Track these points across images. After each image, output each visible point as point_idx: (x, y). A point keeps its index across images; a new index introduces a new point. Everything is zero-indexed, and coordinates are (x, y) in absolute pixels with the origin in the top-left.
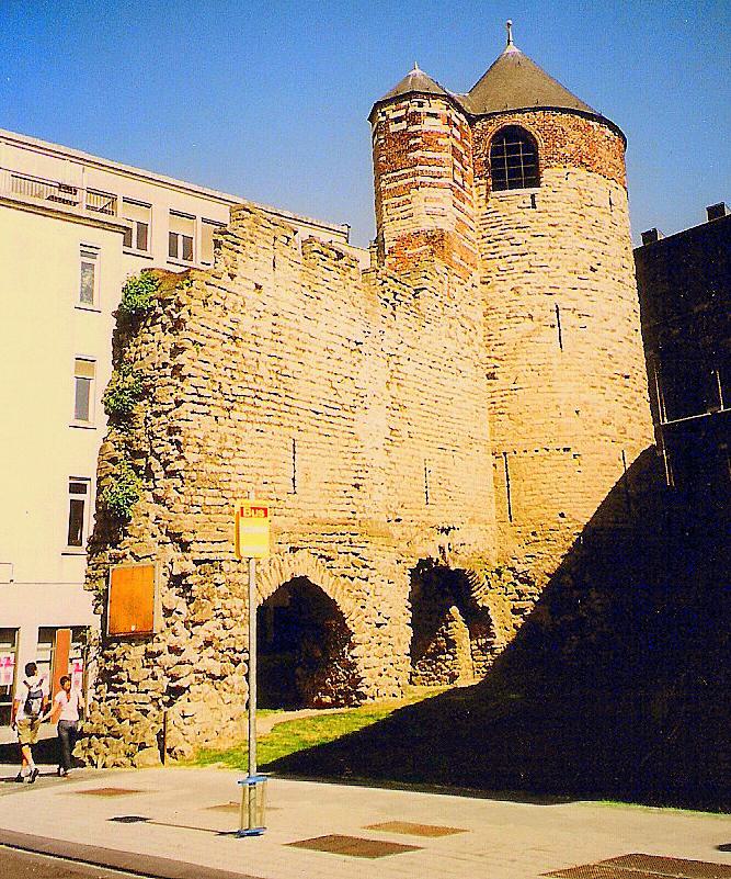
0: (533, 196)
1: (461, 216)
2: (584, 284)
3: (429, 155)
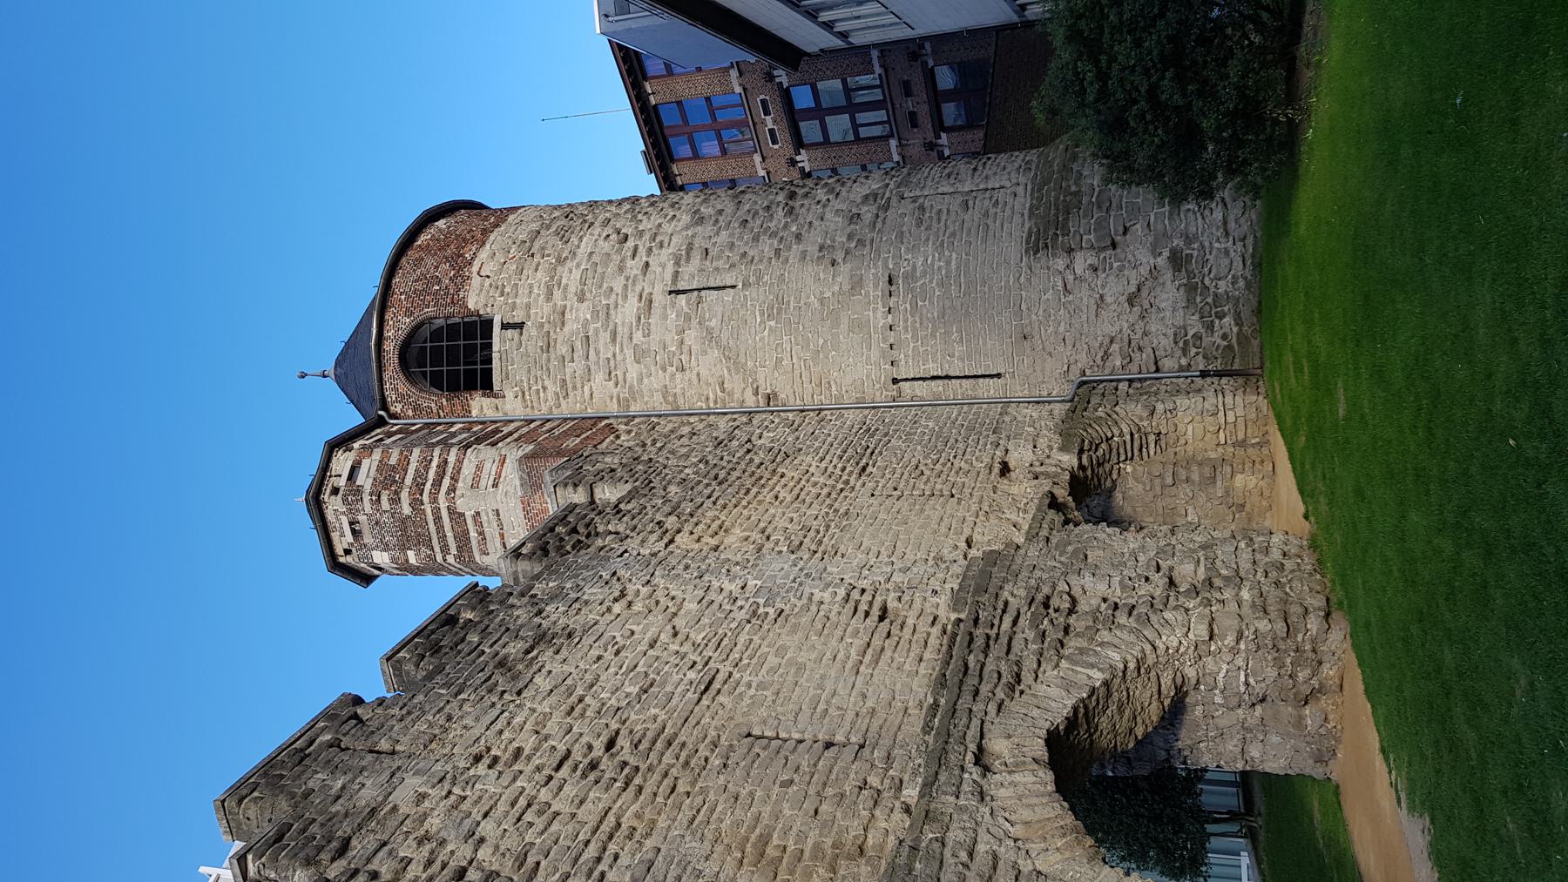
0: (505, 326)
1: (516, 435)
2: (642, 250)
3: (409, 480)
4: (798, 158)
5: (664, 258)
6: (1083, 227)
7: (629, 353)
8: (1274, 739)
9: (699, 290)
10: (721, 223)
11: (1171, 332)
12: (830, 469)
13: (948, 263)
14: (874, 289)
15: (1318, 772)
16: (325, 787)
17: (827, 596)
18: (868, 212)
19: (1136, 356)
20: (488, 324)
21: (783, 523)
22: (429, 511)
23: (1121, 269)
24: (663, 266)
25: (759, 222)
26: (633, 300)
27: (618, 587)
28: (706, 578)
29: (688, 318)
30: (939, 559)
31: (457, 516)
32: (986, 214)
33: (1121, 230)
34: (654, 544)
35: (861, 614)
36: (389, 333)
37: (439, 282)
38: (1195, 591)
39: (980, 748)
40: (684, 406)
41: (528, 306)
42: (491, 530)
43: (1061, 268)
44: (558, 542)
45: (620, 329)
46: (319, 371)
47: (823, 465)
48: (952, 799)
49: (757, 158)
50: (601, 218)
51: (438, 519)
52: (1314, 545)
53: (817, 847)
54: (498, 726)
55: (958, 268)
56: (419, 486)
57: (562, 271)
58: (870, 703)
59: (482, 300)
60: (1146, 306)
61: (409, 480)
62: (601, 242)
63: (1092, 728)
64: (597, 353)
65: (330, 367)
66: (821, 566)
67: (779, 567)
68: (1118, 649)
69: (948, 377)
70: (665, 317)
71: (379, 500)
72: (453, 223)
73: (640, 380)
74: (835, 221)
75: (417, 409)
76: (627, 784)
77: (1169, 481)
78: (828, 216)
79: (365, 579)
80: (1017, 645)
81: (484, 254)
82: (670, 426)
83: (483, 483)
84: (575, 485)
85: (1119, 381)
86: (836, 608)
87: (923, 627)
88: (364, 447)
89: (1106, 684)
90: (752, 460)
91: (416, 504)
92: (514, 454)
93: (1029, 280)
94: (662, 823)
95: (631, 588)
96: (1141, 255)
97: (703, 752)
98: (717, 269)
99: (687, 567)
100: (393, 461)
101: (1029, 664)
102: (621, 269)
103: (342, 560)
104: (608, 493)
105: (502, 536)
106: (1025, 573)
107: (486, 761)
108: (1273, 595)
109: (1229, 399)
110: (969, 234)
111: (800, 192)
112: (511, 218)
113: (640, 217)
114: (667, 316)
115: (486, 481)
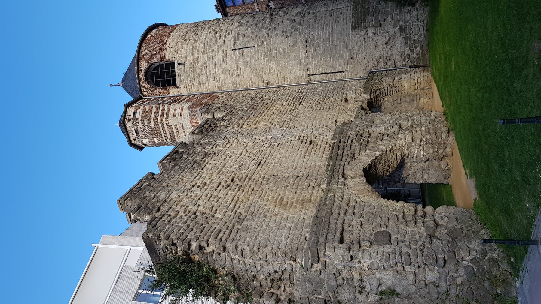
0: (179, 64)
2: (222, 36)
3: (153, 116)
4: (270, 4)
5: (230, 38)
6: (370, 20)
7: (220, 71)
8: (432, 172)
9: (242, 48)
10: (249, 25)
11: (400, 54)
12: (290, 104)
13: (325, 34)
14: (301, 44)
15: (445, 182)
17: (293, 139)
18: (298, 18)
19: (388, 62)
20: (172, 65)
21: (276, 120)
22: (160, 125)
23: (383, 33)
24: (230, 41)
25: (261, 24)
27: (227, 140)
28: (254, 136)
29: (239, 58)
30: (327, 127)
31: (169, 126)
32: (338, 17)
33: (383, 20)
34: (236, 128)
35: (304, 143)
37: (156, 51)
38: (407, 129)
39: (343, 173)
40: (239, 88)
41: (186, 57)
42: (181, 130)
43: (363, 34)
44: (206, 129)
45: (217, 63)
46: (116, 84)
47: (287, 103)
48: (336, 186)
49: (256, 5)
51: (163, 127)
52: (445, 114)
53: (297, 201)
54: (198, 177)
55: (329, 36)
56: (156, 117)
57: (197, 45)
58: (309, 165)
59: (171, 56)
60: (392, 45)
61: (153, 116)
62: (208, 34)
63: (376, 169)
65: (120, 82)
66: (290, 131)
67: (277, 132)
68: (384, 146)
69: (326, 73)
70: (232, 58)
71: (144, 122)
72: (157, 32)
73: (225, 80)
74: (287, 22)
75: (152, 93)
76: (239, 190)
77: (399, 102)
78: (284, 21)
80: (353, 147)
81: (170, 40)
82: (236, 94)
83: (177, 115)
84: (208, 113)
85: (383, 71)
86: (296, 142)
87: (323, 145)
88: (137, 106)
89: (381, 155)
90: (264, 103)
91: (156, 123)
92: (186, 106)
93: (353, 39)
94: (251, 198)
95: (231, 140)
96: (390, 28)
97: (260, 180)
98: (248, 41)
99: (248, 134)
100: (147, 110)
101: (357, 151)
102: (216, 43)
103: (133, 142)
104: (218, 115)
105: (184, 132)
106: (354, 128)
107: (196, 186)
108: (431, 128)
109: (419, 74)
110: (332, 24)
111: (274, 13)
112: (177, 28)
113: (221, 25)
114: (233, 57)
115: (178, 114)
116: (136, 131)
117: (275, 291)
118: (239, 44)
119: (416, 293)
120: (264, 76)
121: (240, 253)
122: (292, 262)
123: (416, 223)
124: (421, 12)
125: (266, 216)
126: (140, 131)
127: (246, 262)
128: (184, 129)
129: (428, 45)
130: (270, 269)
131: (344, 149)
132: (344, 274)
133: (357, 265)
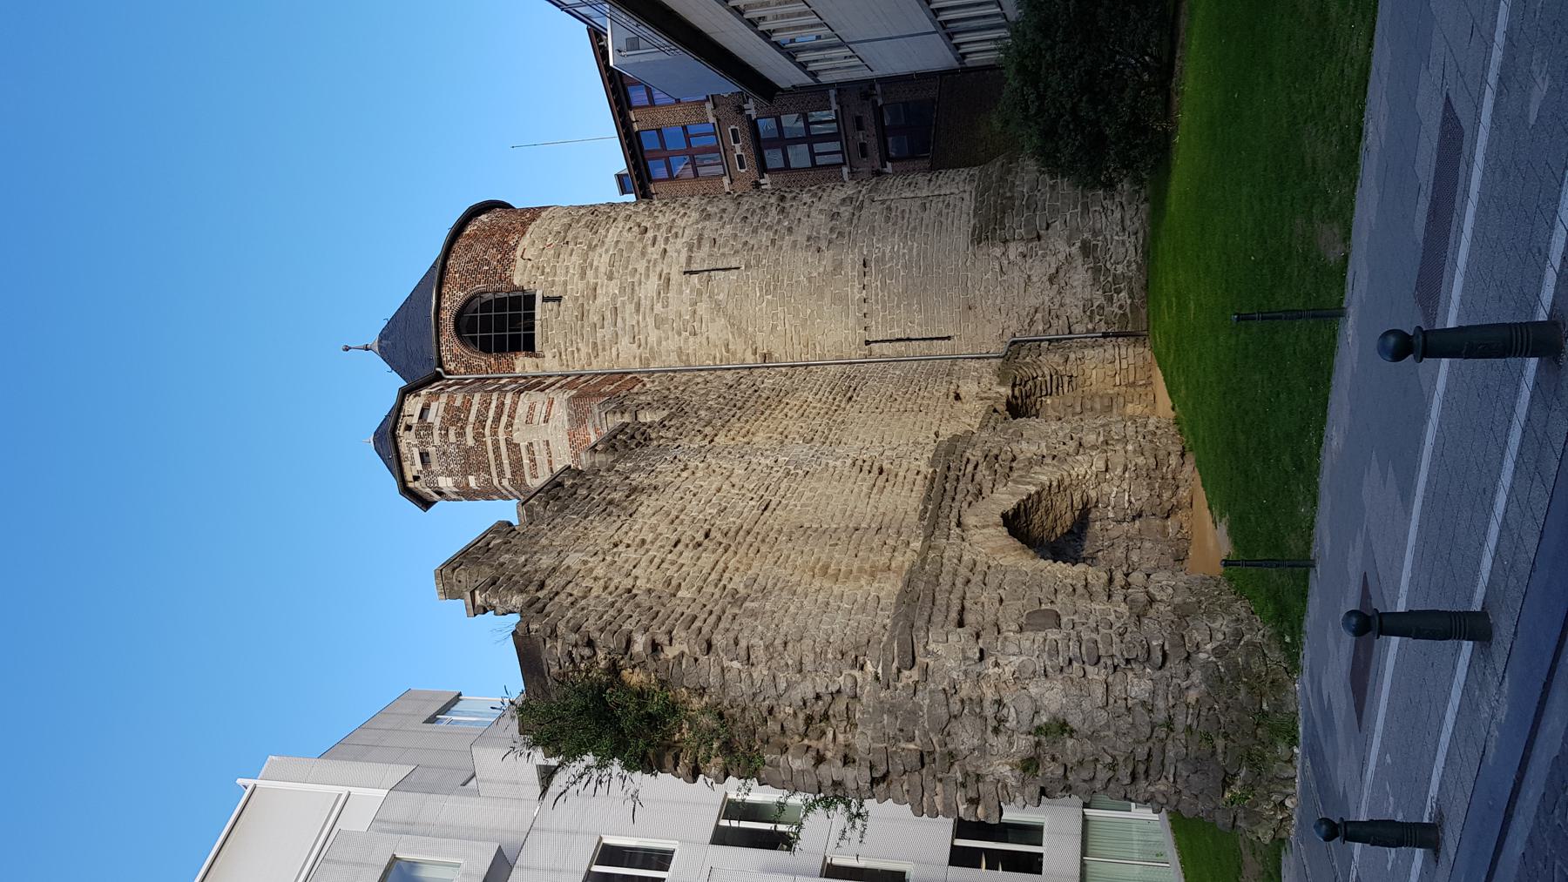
0: (546, 299)
2: (661, 241)
3: (472, 418)
6: (1015, 223)
7: (650, 321)
8: (1148, 545)
11: (1081, 304)
13: (911, 250)
14: (851, 270)
16: (511, 561)
18: (846, 211)
19: (1055, 322)
20: (527, 301)
21: (795, 428)
22: (489, 443)
24: (679, 252)
26: (654, 279)
29: (700, 293)
30: (916, 443)
31: (513, 447)
32: (940, 214)
36: (446, 304)
37: (488, 264)
38: (1094, 447)
40: (695, 363)
41: (565, 283)
42: (541, 458)
44: (626, 442)
46: (362, 344)
49: (726, 180)
50: (623, 214)
51: (497, 449)
52: (1177, 421)
53: (861, 570)
54: (624, 529)
56: (481, 422)
58: (882, 510)
59: (526, 278)
61: (472, 418)
63: (1029, 523)
64: (624, 320)
65: (373, 339)
67: (800, 450)
68: (1045, 476)
69: (909, 339)
70: (681, 292)
72: (487, 222)
73: (659, 343)
74: (819, 218)
75: (469, 368)
77: (1078, 409)
78: (814, 214)
79: (425, 503)
80: (978, 477)
81: (525, 242)
83: (536, 419)
89: (1038, 493)
91: (479, 437)
92: (561, 399)
94: (756, 564)
95: (691, 465)
96: (1059, 246)
98: (723, 254)
100: (458, 403)
102: (643, 254)
103: (411, 485)
105: (550, 462)
108: (1147, 446)
109: (1123, 351)
111: (789, 196)
114: (683, 292)
115: (538, 417)
116: (424, 457)
117: (814, 743)
118: (701, 260)
119: (1108, 726)
120: (759, 338)
121: (743, 653)
122: (857, 673)
123: (1109, 597)
124: (1130, 213)
125: (794, 593)
126: (433, 458)
127: (755, 675)
128: (549, 454)
129: (1146, 287)
130: (806, 689)
131: (958, 479)
132: (966, 690)
133: (991, 671)
